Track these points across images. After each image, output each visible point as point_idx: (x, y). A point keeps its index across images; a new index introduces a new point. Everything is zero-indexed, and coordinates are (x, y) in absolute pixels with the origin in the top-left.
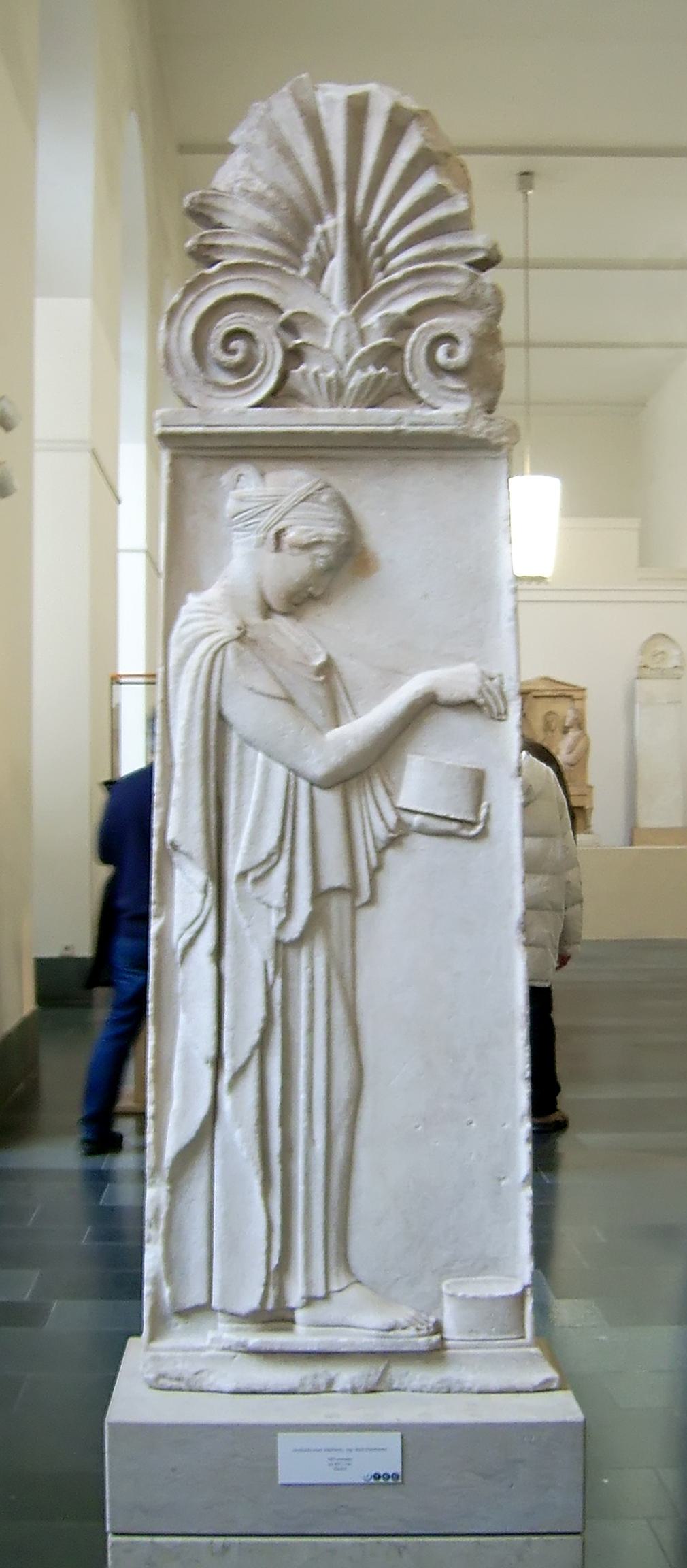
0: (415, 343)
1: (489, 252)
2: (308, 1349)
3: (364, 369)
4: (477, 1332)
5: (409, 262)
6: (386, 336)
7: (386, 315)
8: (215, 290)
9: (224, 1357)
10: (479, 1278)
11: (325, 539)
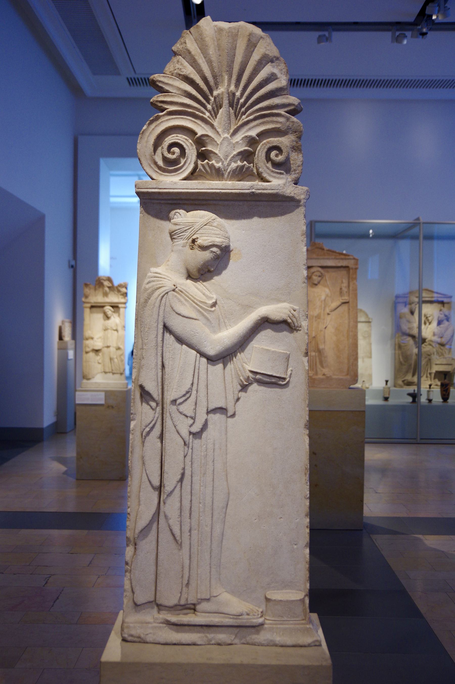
1: (297, 106)
3: (235, 162)
4: (282, 617)
5: (257, 111)
6: (246, 146)
7: (246, 137)
8: (164, 123)
9: (160, 627)
10: (284, 591)
11: (216, 243)
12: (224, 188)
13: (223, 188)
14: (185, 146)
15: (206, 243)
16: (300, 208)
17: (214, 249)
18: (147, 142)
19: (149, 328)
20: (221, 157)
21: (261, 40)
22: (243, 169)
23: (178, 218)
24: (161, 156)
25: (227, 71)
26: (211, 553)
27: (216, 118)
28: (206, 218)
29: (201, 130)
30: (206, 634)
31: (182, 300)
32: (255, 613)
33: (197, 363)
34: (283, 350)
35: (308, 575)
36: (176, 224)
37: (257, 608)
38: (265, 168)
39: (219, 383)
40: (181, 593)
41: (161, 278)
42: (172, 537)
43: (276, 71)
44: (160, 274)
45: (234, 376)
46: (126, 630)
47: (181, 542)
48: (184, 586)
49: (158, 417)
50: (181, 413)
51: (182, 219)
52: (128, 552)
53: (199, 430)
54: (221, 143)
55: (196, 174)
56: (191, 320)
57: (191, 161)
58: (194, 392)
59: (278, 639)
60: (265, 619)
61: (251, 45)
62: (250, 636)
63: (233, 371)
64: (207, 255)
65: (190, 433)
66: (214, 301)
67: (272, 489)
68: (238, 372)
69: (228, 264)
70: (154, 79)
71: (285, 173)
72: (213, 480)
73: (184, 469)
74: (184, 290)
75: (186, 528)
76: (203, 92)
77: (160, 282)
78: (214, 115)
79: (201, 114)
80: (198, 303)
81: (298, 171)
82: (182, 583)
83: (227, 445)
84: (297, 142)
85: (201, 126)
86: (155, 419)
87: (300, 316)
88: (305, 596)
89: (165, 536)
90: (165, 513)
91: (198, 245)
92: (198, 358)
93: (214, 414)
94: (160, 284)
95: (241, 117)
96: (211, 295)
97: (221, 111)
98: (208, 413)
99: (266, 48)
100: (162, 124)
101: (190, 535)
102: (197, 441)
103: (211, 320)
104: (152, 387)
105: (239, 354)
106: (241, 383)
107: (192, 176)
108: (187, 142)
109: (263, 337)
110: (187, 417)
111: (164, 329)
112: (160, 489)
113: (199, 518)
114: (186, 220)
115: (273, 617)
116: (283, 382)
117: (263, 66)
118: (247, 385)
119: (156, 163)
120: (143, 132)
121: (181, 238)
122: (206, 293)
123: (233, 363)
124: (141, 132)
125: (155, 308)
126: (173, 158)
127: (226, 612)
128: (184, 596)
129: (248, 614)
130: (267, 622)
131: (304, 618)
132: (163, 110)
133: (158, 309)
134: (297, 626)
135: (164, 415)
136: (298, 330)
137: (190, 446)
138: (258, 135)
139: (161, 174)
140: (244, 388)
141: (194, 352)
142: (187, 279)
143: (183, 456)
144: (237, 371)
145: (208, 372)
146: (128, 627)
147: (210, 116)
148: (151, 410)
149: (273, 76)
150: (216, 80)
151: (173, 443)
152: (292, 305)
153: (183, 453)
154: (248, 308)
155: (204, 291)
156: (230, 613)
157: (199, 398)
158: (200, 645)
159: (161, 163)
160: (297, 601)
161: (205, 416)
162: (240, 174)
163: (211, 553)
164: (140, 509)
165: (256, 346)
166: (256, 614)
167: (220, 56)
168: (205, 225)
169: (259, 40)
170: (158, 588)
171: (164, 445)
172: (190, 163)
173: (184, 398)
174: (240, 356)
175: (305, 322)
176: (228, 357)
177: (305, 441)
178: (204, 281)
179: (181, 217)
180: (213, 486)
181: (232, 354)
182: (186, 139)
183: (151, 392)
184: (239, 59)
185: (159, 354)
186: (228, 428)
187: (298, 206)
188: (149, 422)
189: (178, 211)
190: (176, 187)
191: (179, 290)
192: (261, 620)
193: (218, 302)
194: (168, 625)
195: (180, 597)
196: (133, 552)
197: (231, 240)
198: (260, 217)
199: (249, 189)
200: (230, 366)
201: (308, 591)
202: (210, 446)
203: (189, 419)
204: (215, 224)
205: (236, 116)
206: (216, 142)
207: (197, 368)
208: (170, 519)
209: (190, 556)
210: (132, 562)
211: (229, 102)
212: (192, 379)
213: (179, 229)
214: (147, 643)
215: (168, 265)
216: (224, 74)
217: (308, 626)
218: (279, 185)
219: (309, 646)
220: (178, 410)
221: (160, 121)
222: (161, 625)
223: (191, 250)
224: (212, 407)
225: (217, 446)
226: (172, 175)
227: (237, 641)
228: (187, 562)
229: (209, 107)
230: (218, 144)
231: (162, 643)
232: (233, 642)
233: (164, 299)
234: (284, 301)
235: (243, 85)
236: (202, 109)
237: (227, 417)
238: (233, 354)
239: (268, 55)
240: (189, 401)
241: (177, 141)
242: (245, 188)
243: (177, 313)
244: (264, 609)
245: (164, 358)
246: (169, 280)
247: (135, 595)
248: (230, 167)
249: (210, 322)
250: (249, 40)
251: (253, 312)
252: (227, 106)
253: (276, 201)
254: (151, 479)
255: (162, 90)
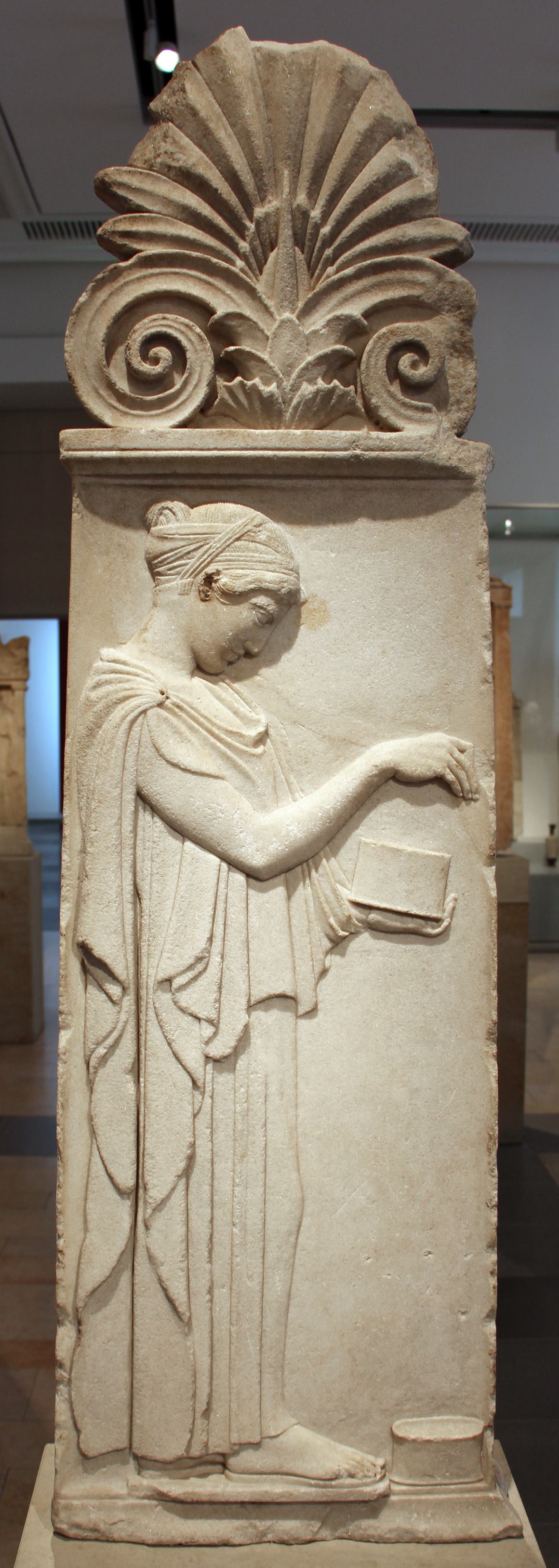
0: (371, 351)
1: (461, 245)
2: (239, 1500)
3: (312, 381)
4: (431, 1476)
5: (364, 255)
6: (337, 342)
7: (337, 318)
8: (132, 287)
9: (144, 1507)
10: (435, 1418)
11: (265, 585)
12: (285, 446)
13: (282, 445)
14: (185, 342)
15: (239, 586)
16: (474, 494)
17: (262, 600)
18: (89, 333)
19: (100, 802)
20: (276, 369)
21: (371, 84)
22: (331, 398)
23: (168, 522)
24: (125, 368)
25: (289, 158)
26: (261, 1340)
27: (261, 272)
28: (240, 522)
29: (223, 302)
30: (253, 1521)
31: (183, 728)
32: (369, 1471)
33: (222, 885)
34: (433, 850)
35: (493, 1383)
36: (163, 538)
37: (371, 1458)
38: (385, 398)
39: (274, 934)
40: (192, 1431)
41: (128, 673)
42: (166, 1306)
43: (407, 158)
44: (124, 663)
45: (313, 917)
46: (63, 1515)
47: (190, 1318)
48: (198, 1415)
49: (126, 1022)
50: (182, 1010)
51: (178, 525)
52: (63, 1339)
53: (228, 1051)
54: (275, 335)
55: (212, 411)
56: (205, 779)
57: (199, 381)
58: (215, 959)
59: (423, 1526)
60: (391, 1481)
61: (348, 95)
62: (356, 1523)
63: (311, 904)
64: (243, 615)
65: (207, 1058)
66: (262, 729)
67: (406, 1187)
68: (325, 905)
69: (295, 636)
70: (106, 179)
71: (434, 409)
72: (265, 1170)
73: (193, 1145)
74: (186, 703)
75: (200, 1284)
76: (229, 211)
77: (127, 686)
78: (255, 266)
79: (224, 264)
80: (223, 736)
81: (465, 405)
82: (194, 1410)
83: (296, 1084)
84: (462, 333)
85: (223, 293)
86: (120, 1026)
87: (477, 764)
88: (485, 1428)
89: (150, 1303)
90: (148, 1249)
91: (219, 589)
92: (224, 874)
93: (266, 1010)
94: (126, 689)
95: (324, 269)
96: (253, 714)
97: (272, 255)
98: (251, 1007)
99: (383, 102)
100: (126, 289)
101: (211, 1301)
102: (224, 1080)
103: (255, 777)
104: (110, 948)
105: (324, 861)
106: (331, 934)
107: (204, 415)
108: (190, 333)
109: (385, 819)
110: (199, 1019)
111: (136, 802)
112: (135, 1193)
113: (231, 1259)
114: (189, 527)
115: (410, 1476)
116: (433, 928)
117: (376, 145)
118: (344, 938)
119: (111, 386)
120: (79, 309)
121: (178, 573)
122: (242, 709)
123: (312, 884)
124: (75, 310)
125: (114, 751)
126: (154, 372)
127: (299, 1471)
128: (200, 1437)
129: (352, 1476)
130: (395, 1488)
131: (482, 1476)
132: (127, 254)
133: (121, 754)
134: (467, 1495)
135: (142, 1017)
136: (472, 799)
137: (208, 1089)
138: (367, 314)
139: (126, 414)
140: (337, 943)
141: (214, 860)
142: (192, 674)
143: (190, 1115)
144: (321, 903)
145: (250, 906)
146: (67, 1508)
147: (246, 268)
148: (110, 1004)
149: (401, 170)
150: (261, 180)
151: (165, 1082)
152: (455, 739)
153: (190, 1108)
154: (345, 746)
155: (236, 705)
156: (310, 1475)
157: (227, 973)
158: (240, 1545)
159: (123, 385)
160: (466, 1440)
161: (244, 1018)
162: (324, 412)
163: (261, 1340)
164: (87, 1241)
165: (368, 841)
166: (370, 1474)
167: (270, 121)
168: (238, 539)
169: (367, 84)
170: (137, 1421)
171: (142, 1090)
172: (196, 386)
173: (190, 975)
174: (329, 865)
175: (488, 779)
176: (299, 869)
177: (487, 1071)
178: (237, 679)
179: (178, 520)
180: (265, 1184)
181: (307, 861)
182: (187, 326)
183: (108, 961)
184: (317, 127)
185: (127, 865)
186: (300, 1043)
187: (468, 491)
188: (104, 1034)
189: (169, 504)
190: (162, 445)
191: (174, 704)
192: (381, 1487)
193: (271, 732)
194: (163, 1503)
195: (190, 1442)
196: (74, 1339)
197: (301, 575)
198: (374, 517)
199: (345, 449)
200: (303, 892)
201: (492, 1417)
202: (257, 1089)
203: (204, 1024)
204: (262, 537)
205: (311, 269)
206: (262, 331)
207: (221, 898)
208: (162, 1264)
209: (212, 1347)
210: (72, 1362)
211: (295, 234)
212: (209, 926)
213: (172, 550)
214: (114, 1541)
215: (145, 641)
216: (280, 165)
217: (491, 1495)
218: (422, 438)
219: (496, 1539)
220: (175, 1003)
221: (122, 281)
222: (146, 1501)
223: (203, 604)
224: (260, 993)
225: (273, 1089)
226: (152, 416)
227: (325, 1533)
228: (204, 1361)
229: (244, 246)
230: (267, 338)
231: (150, 1542)
232: (318, 1537)
233: (136, 728)
234: (436, 728)
235: (329, 192)
236: (227, 251)
237: (298, 1017)
238: (311, 862)
239: (391, 119)
240: (202, 981)
241: (164, 329)
242: (338, 445)
243: (168, 762)
244: (389, 1458)
245: (139, 874)
246: (148, 679)
247: (82, 1437)
248: (299, 393)
249: (253, 782)
250: (342, 82)
251: (359, 754)
252: (290, 243)
253: (414, 479)
254: (112, 1170)
255: (124, 207)
